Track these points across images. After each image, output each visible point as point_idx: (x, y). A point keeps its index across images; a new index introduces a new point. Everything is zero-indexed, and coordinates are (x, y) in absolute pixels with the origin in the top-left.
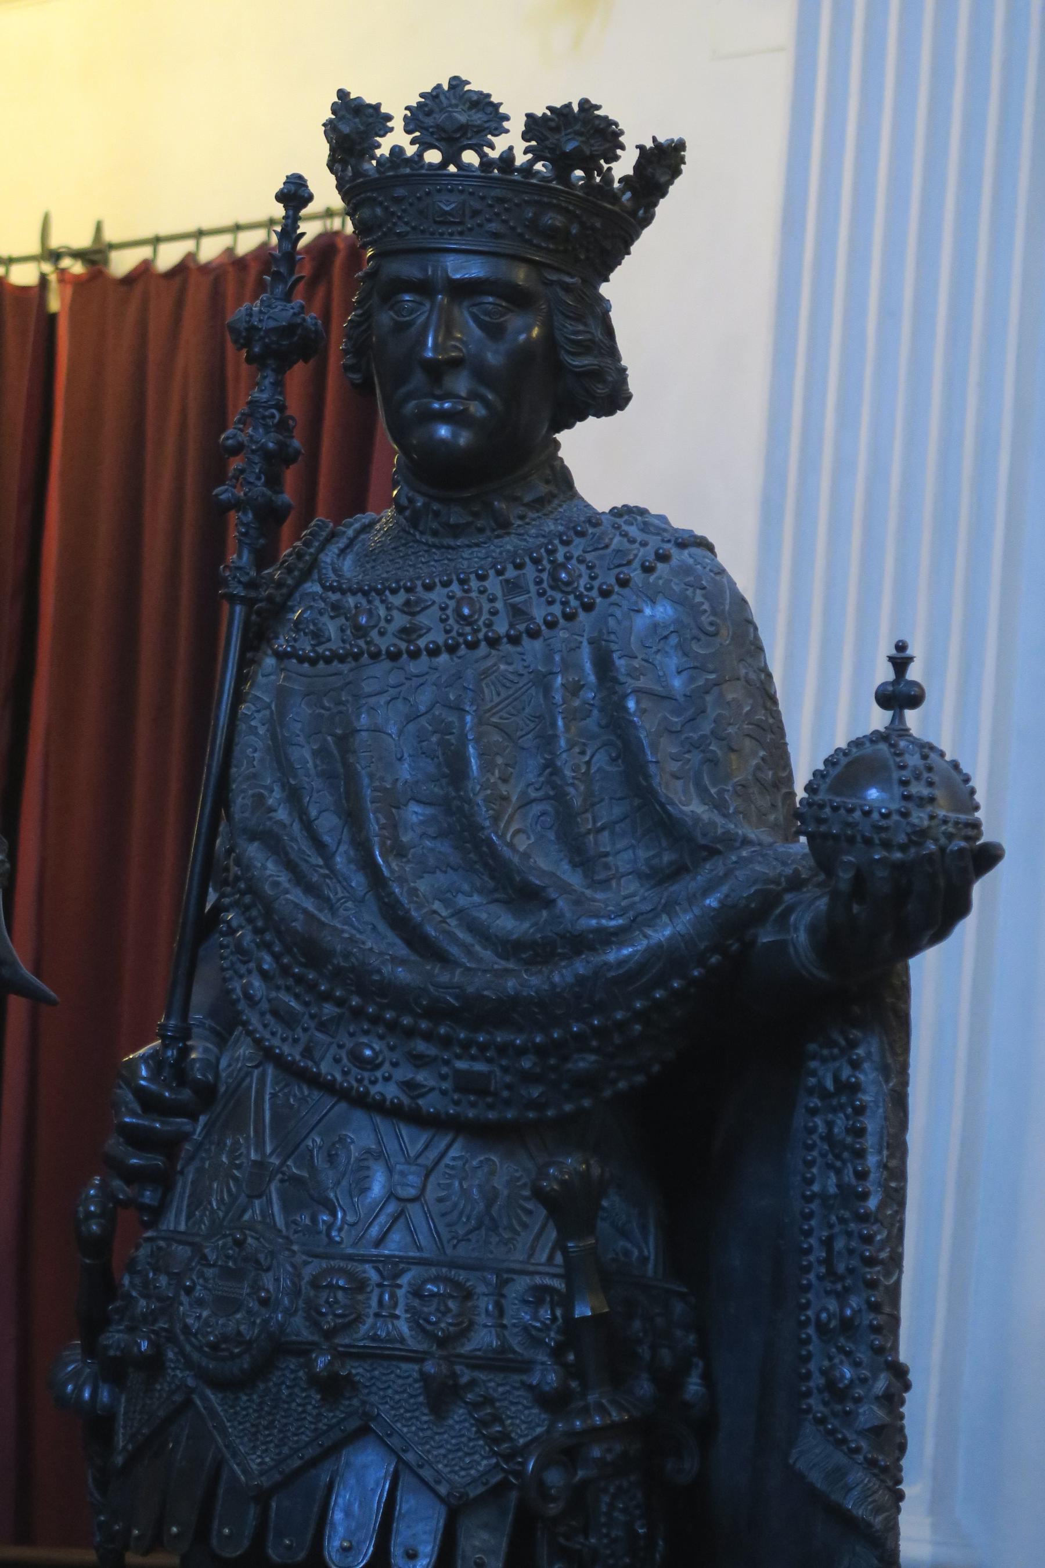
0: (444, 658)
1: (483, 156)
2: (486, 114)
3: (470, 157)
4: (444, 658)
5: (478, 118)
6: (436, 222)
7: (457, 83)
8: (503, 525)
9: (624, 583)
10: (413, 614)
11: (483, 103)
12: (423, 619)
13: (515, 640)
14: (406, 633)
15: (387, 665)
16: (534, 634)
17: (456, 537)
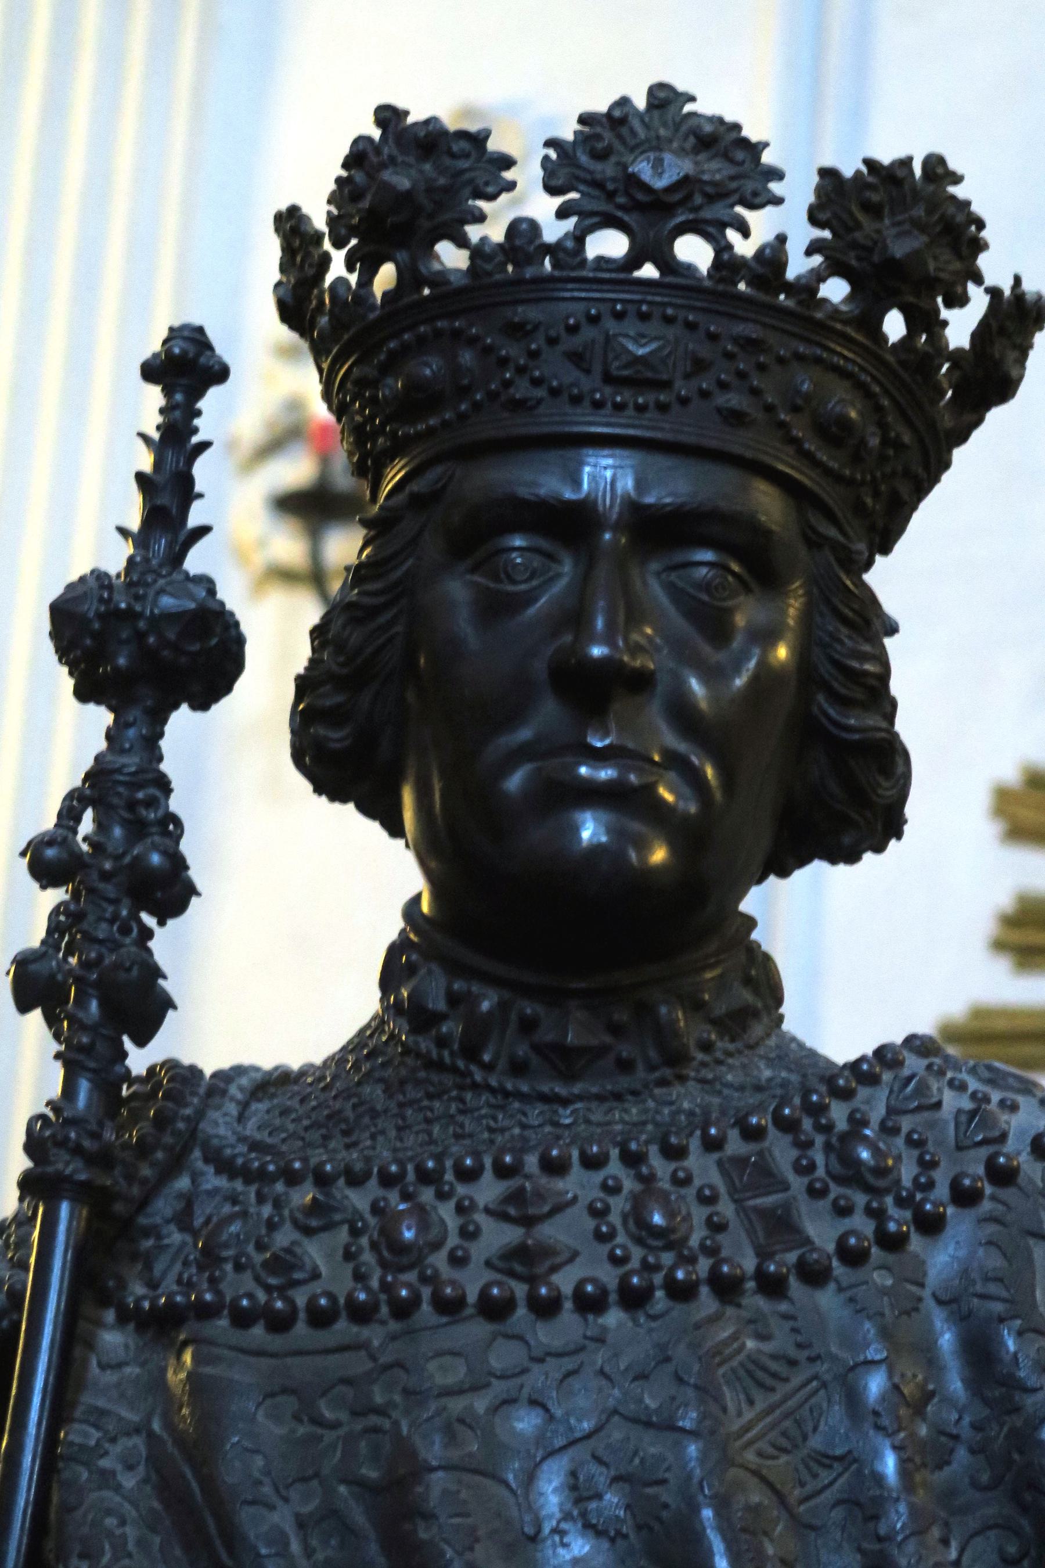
0: (614, 1317)
1: (723, 249)
2: (727, 166)
3: (694, 251)
4: (614, 1317)
5: (714, 170)
6: (608, 379)
7: (665, 98)
8: (674, 1059)
9: (1003, 1176)
10: (528, 1222)
11: (724, 142)
12: (551, 1232)
13: (772, 1286)
14: (525, 1260)
15: (478, 1329)
16: (814, 1275)
17: (569, 1077)
